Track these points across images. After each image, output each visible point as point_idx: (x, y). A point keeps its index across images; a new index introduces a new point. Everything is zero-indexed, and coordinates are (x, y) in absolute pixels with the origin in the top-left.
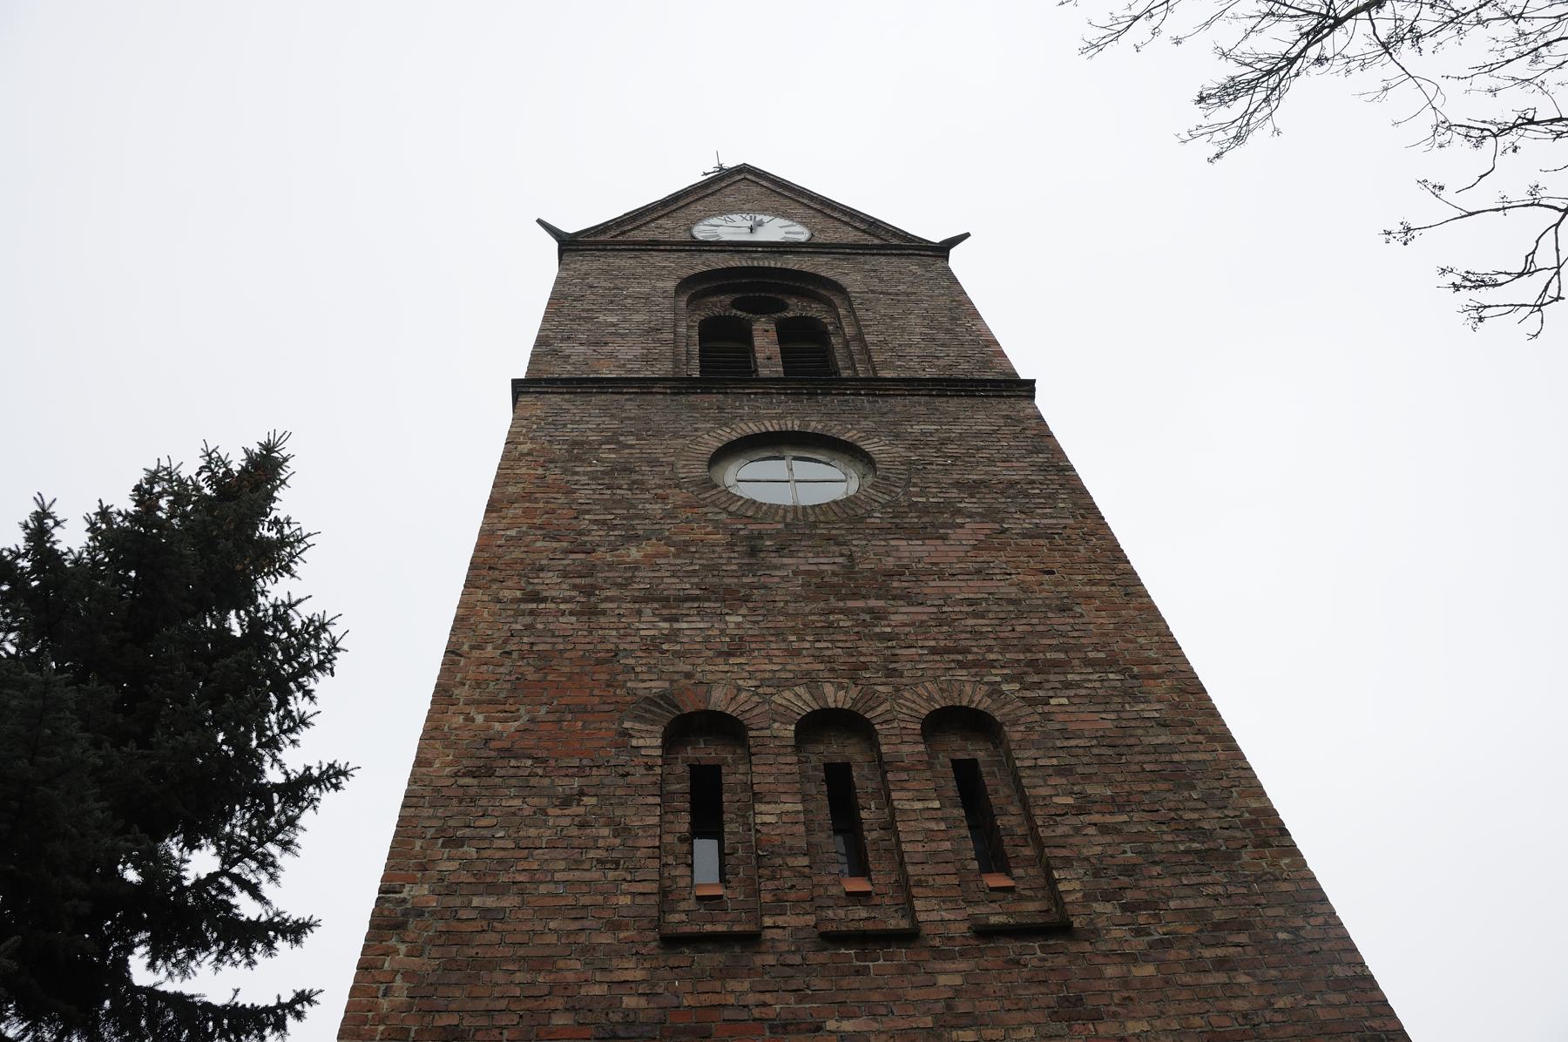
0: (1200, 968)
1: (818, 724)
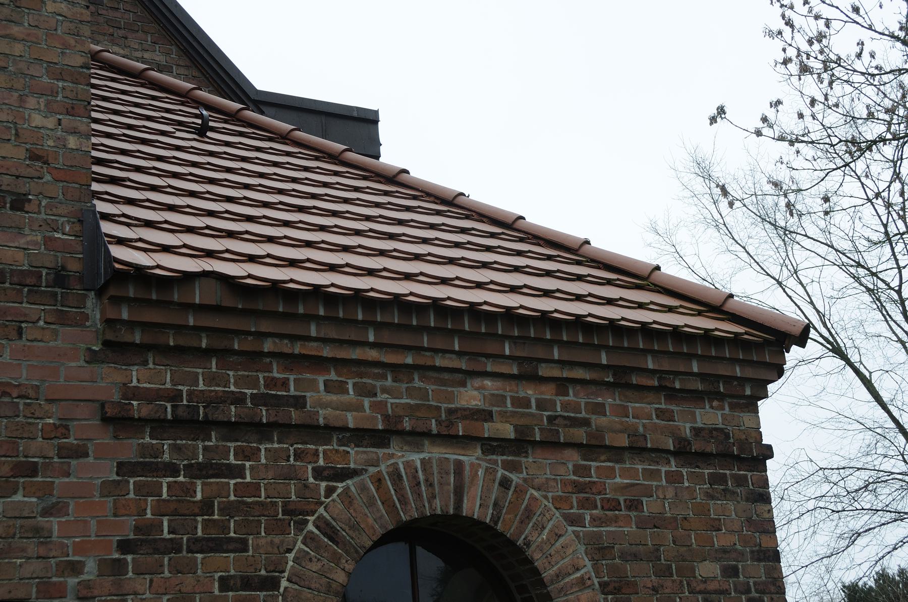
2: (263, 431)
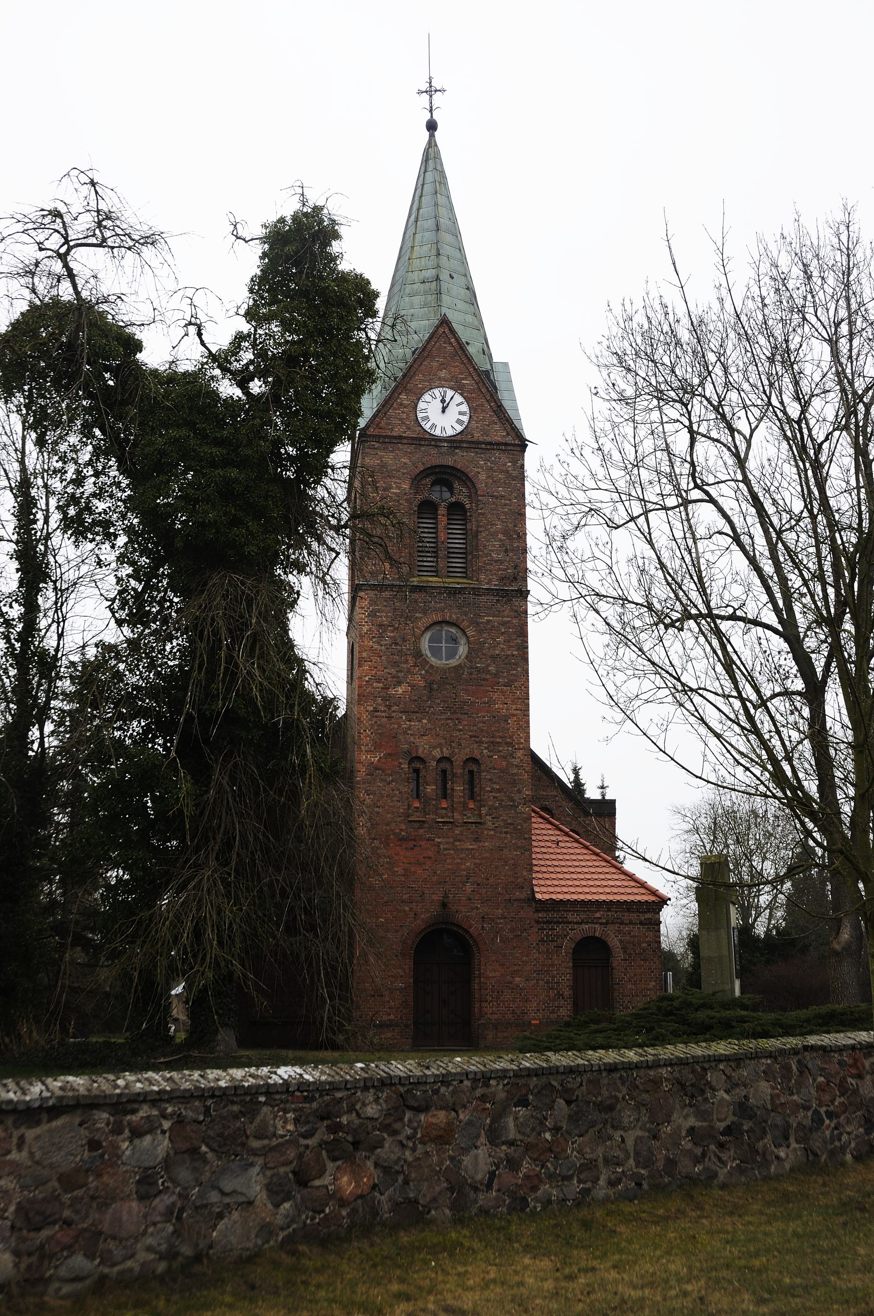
0: (501, 833)
1: (443, 759)
2: (560, 923)
